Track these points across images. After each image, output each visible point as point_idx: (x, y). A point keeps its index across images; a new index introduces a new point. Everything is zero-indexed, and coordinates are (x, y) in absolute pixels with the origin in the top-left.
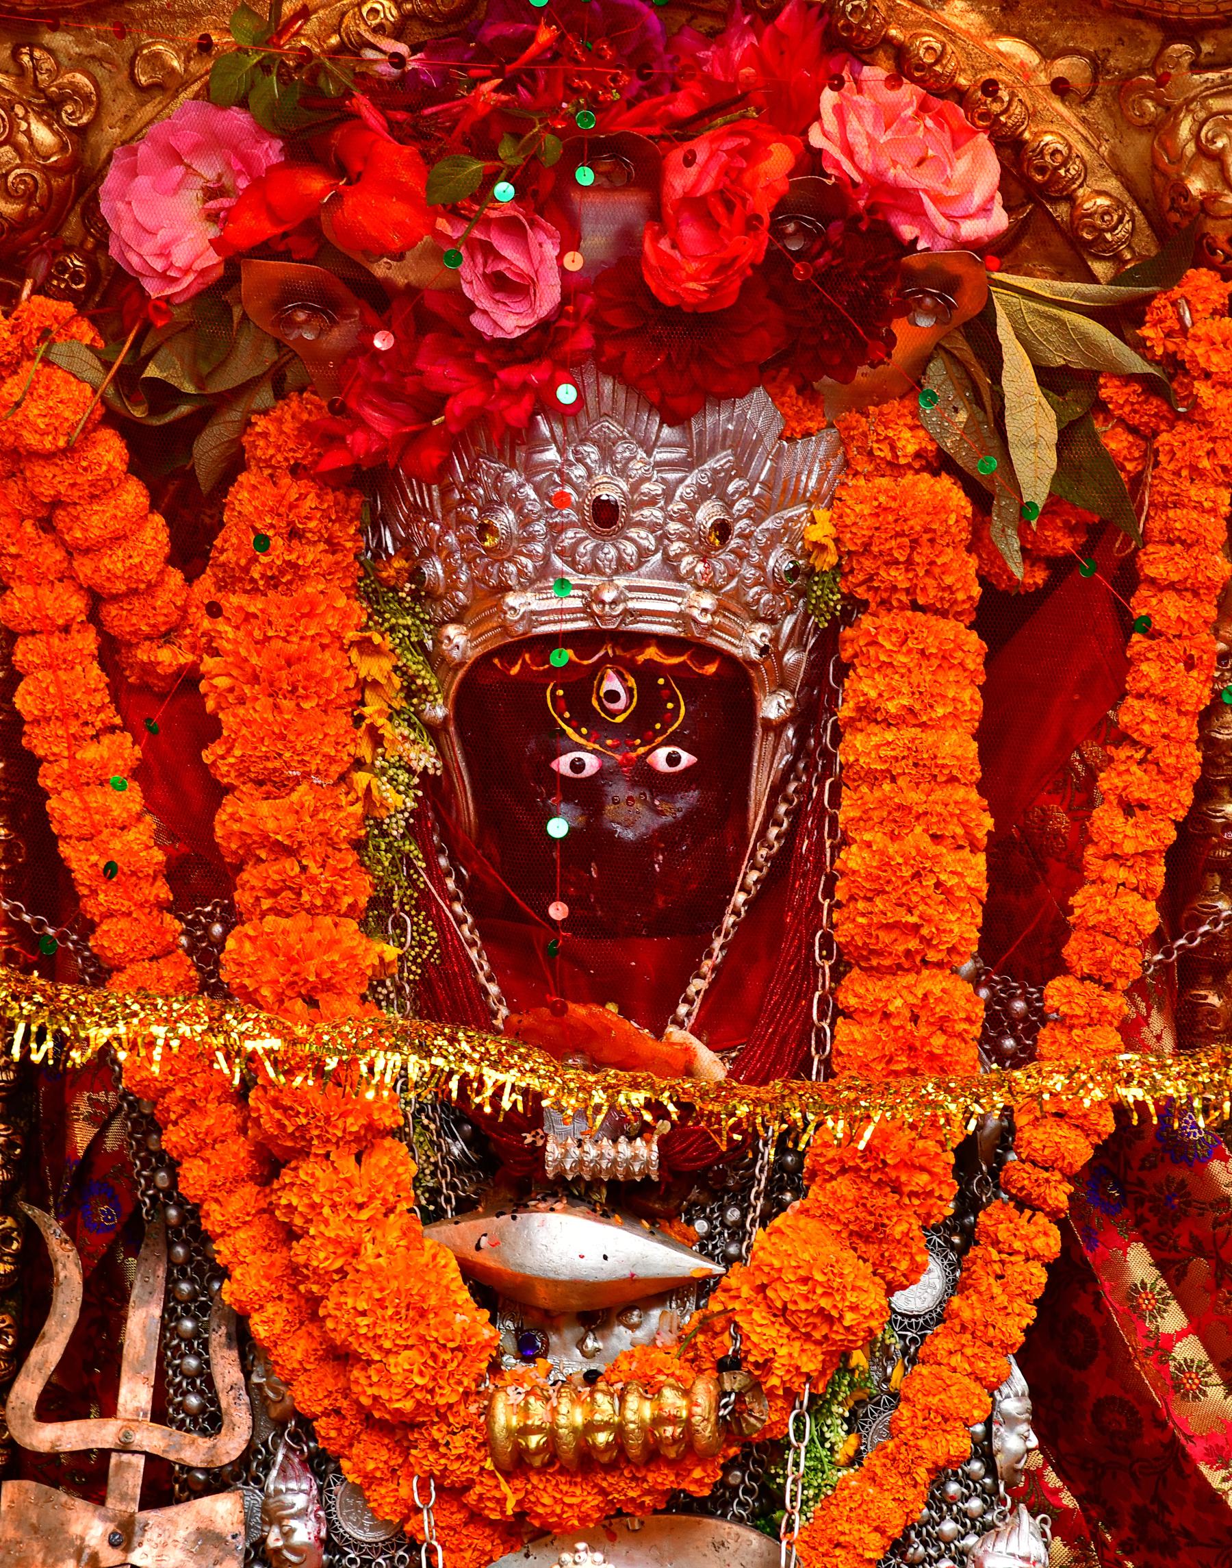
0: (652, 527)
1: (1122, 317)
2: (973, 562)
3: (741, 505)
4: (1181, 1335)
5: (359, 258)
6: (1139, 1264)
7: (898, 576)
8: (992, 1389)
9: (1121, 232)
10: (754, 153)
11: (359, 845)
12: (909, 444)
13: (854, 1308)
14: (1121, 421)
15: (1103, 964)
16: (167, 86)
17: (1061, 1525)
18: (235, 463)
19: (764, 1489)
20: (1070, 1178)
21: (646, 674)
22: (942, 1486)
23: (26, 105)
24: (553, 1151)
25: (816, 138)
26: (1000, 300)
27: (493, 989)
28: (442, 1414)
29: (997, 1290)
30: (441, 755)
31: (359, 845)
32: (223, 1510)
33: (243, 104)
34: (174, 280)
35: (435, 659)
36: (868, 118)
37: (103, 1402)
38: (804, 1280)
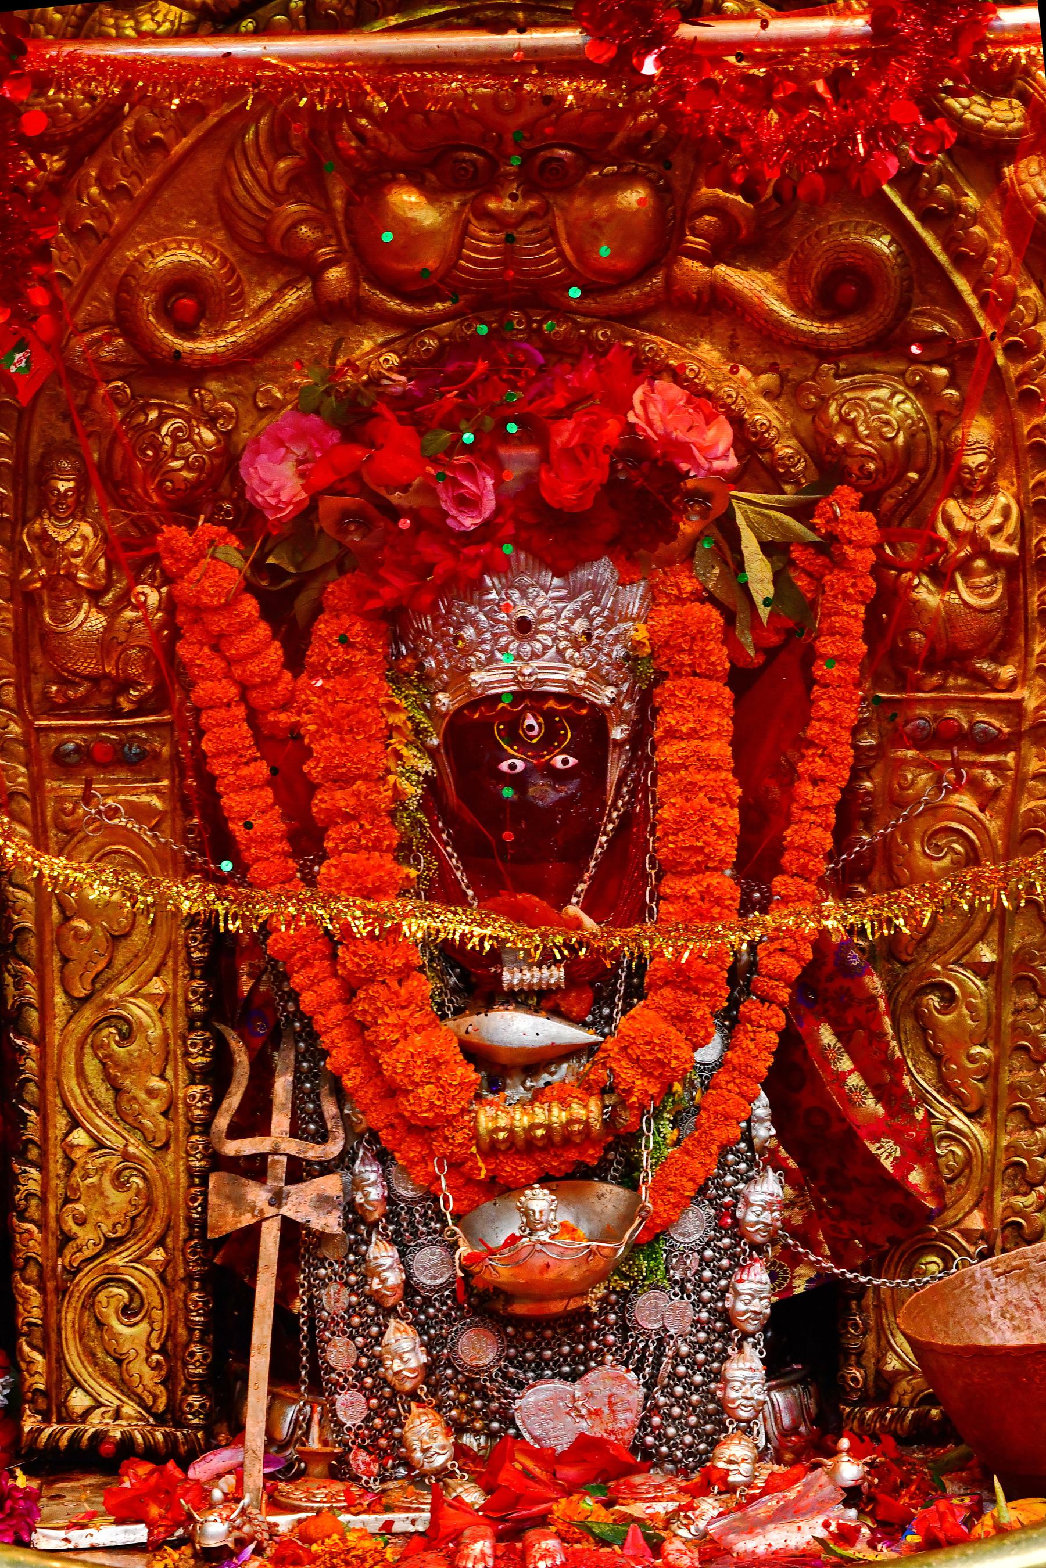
0: (550, 633)
1: (801, 512)
2: (725, 651)
3: (598, 621)
4: (851, 1072)
5: (383, 492)
6: (827, 1036)
7: (686, 658)
8: (750, 1101)
9: (800, 467)
10: (599, 424)
11: (392, 814)
12: (688, 586)
13: (676, 1058)
14: (804, 571)
15: (804, 866)
16: (273, 407)
17: (789, 1178)
18: (318, 609)
19: (628, 1161)
20: (788, 985)
21: (548, 716)
22: (725, 1157)
23: (198, 420)
24: (506, 976)
25: (631, 418)
26: (735, 504)
27: (470, 892)
28: (450, 1121)
29: (752, 1046)
30: (436, 765)
31: (392, 814)
32: (331, 1185)
33: (317, 412)
34: (283, 510)
35: (432, 713)
36: (660, 406)
37: (263, 1129)
38: (648, 1043)
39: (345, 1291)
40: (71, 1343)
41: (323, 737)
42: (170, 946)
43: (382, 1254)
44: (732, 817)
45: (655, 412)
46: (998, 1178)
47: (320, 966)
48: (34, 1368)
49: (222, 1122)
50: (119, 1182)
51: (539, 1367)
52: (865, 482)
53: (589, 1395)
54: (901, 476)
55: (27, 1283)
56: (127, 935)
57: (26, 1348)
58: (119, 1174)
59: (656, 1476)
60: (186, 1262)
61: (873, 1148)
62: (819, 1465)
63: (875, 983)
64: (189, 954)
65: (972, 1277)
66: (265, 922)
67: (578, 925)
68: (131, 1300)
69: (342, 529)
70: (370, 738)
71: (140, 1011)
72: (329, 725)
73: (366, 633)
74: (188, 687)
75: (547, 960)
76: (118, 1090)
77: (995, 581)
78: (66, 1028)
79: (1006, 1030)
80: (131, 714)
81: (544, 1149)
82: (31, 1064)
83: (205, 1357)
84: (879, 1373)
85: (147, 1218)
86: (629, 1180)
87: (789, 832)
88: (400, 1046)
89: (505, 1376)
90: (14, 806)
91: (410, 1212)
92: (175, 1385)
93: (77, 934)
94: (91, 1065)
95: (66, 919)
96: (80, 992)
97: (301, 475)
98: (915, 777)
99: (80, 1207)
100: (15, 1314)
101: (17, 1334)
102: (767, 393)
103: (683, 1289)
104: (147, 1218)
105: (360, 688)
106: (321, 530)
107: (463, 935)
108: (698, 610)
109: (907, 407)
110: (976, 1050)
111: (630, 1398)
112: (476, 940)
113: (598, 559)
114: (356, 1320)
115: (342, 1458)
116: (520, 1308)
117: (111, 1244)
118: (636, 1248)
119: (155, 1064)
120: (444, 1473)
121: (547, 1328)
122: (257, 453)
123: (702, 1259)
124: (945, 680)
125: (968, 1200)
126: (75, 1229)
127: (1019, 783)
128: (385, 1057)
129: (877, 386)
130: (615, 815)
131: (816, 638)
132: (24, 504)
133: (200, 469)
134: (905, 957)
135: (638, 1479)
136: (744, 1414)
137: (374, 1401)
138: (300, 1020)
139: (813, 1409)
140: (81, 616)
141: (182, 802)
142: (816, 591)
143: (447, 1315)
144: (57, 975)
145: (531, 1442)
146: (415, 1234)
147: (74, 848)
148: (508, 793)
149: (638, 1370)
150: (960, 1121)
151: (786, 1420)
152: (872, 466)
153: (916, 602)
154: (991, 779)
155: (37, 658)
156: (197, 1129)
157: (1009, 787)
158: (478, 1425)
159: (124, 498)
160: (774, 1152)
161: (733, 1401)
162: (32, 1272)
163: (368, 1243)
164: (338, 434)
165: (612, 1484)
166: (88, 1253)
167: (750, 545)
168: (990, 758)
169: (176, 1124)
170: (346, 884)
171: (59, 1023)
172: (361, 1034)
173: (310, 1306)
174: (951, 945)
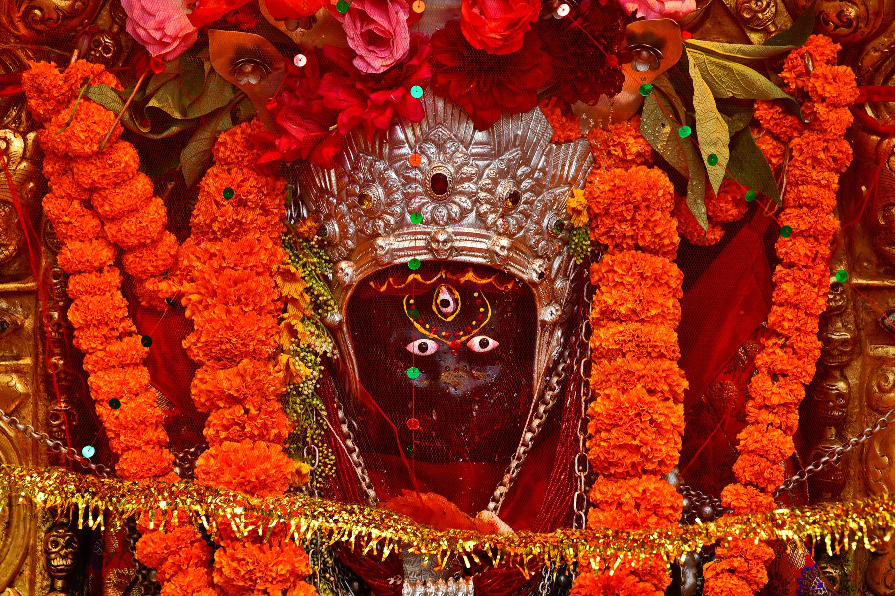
0: (470, 195)
1: (768, 65)
2: (675, 223)
5: (282, 26)
9: (768, 13)
11: (284, 399)
14: (769, 132)
21: (466, 290)
26: (691, 54)
27: (372, 493)
30: (337, 344)
31: (284, 399)
34: (167, 45)
41: (206, 308)
42: (29, 551)
47: (195, 575)
52: (844, 30)
64: (48, 561)
66: (132, 519)
67: (492, 529)
69: (236, 69)
70: (260, 311)
72: (214, 294)
73: (260, 191)
74: (56, 249)
87: (742, 435)
105: (250, 253)
106: (212, 70)
107: (359, 537)
108: (642, 173)
112: (374, 544)
113: (528, 109)
130: (542, 408)
131: (781, 210)
141: (48, 384)
142: (783, 156)
148: (413, 373)
167: (704, 100)
170: (227, 477)
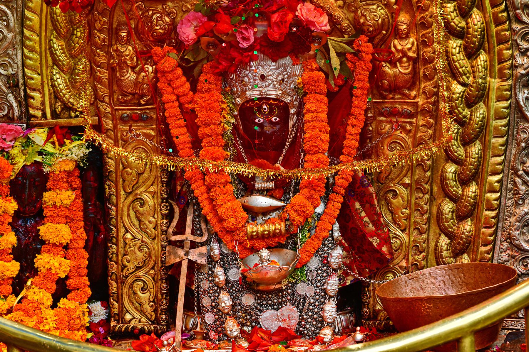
0: (271, 80)
1: (349, 43)
2: (326, 86)
3: (286, 76)
4: (365, 217)
5: (220, 36)
6: (357, 205)
7: (313, 88)
8: (332, 225)
10: (286, 15)
11: (222, 135)
12: (314, 66)
13: (308, 210)
14: (350, 61)
15: (349, 152)
16: (188, 11)
17: (345, 249)
19: (294, 242)
20: (344, 189)
21: (270, 105)
22: (324, 242)
23: (164, 14)
24: (256, 185)
25: (297, 13)
26: (329, 41)
27: (247, 160)
28: (239, 229)
29: (333, 207)
30: (236, 120)
31: (222, 135)
33: (200, 12)
34: (189, 41)
35: (235, 104)
36: (306, 10)
37: (183, 233)
38: (300, 205)
39: (208, 282)
40: (126, 299)
41: (201, 111)
42: (156, 177)
43: (219, 271)
44: (327, 137)
45: (304, 12)
46: (410, 250)
47: (200, 182)
48: (114, 307)
49: (171, 230)
50: (140, 250)
51: (267, 306)
53: (282, 315)
54: (380, 33)
55: (112, 280)
56: (143, 173)
57: (112, 300)
58: (140, 247)
59: (303, 340)
60: (161, 274)
61: (371, 240)
62: (350, 335)
63: (371, 189)
64: (162, 179)
65: (401, 280)
66: (183, 168)
67: (279, 169)
68: (144, 286)
69: (208, 47)
70: (216, 112)
71: (147, 197)
72: (203, 108)
73: (215, 80)
74: (161, 97)
75: (268, 180)
76: (140, 221)
77: (409, 65)
78: (124, 202)
79: (413, 204)
80: (144, 105)
81: (267, 238)
82: (113, 213)
83: (166, 303)
84: (374, 310)
85: (149, 261)
86: (294, 249)
87: (345, 142)
88: (223, 206)
89: (257, 309)
90: (108, 133)
91: (227, 258)
92: (157, 312)
93: (127, 173)
94: (132, 213)
95: (124, 168)
96: (129, 190)
97: (196, 31)
98: (385, 126)
99: (128, 257)
100: (108, 290)
101: (109, 296)
102: (339, 7)
103: (311, 283)
104: (149, 261)
105: (213, 97)
106: (201, 48)
107: (243, 172)
108: (317, 73)
109: (382, 11)
110: (404, 210)
111: (295, 315)
112: (247, 173)
113: (286, 56)
114: (211, 291)
115: (207, 334)
116: (261, 288)
117: (138, 268)
118: (296, 269)
119: (151, 213)
120: (236, 337)
121: (268, 293)
122: (182, 24)
123: (318, 273)
124: (394, 95)
125: (401, 256)
126: (127, 264)
127: (417, 128)
128: (219, 210)
129: (373, 4)
130: (291, 136)
131: (354, 82)
132: (112, 40)
133: (165, 29)
134: (382, 182)
135: (296, 340)
136: (329, 321)
137: (217, 316)
138: (195, 199)
139: (354, 321)
140: (129, 75)
141: (159, 132)
142: (354, 68)
143: (239, 290)
144: (121, 185)
145: (264, 329)
146: (229, 265)
147: (127, 146)
148: (256, 128)
149: (297, 307)
150: (399, 232)
151: (345, 324)
152: (371, 29)
153: (384, 71)
154: (408, 127)
155: (115, 88)
156: (164, 233)
157: (414, 129)
158: (248, 324)
159: (142, 38)
160: (340, 241)
161: (326, 316)
162: (114, 277)
163: (214, 268)
164: (207, 18)
165: (289, 342)
166: (131, 271)
168: (408, 120)
169: (158, 232)
170: (208, 156)
171: (122, 200)
172: (212, 203)
173: (198, 287)
174: (396, 178)
